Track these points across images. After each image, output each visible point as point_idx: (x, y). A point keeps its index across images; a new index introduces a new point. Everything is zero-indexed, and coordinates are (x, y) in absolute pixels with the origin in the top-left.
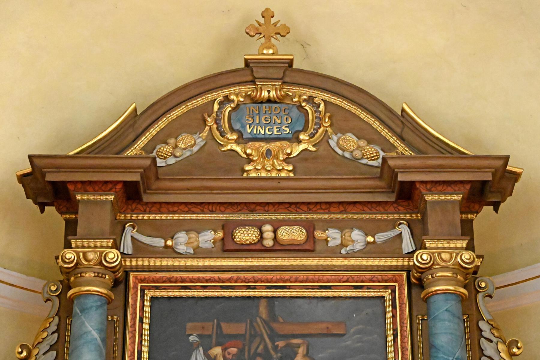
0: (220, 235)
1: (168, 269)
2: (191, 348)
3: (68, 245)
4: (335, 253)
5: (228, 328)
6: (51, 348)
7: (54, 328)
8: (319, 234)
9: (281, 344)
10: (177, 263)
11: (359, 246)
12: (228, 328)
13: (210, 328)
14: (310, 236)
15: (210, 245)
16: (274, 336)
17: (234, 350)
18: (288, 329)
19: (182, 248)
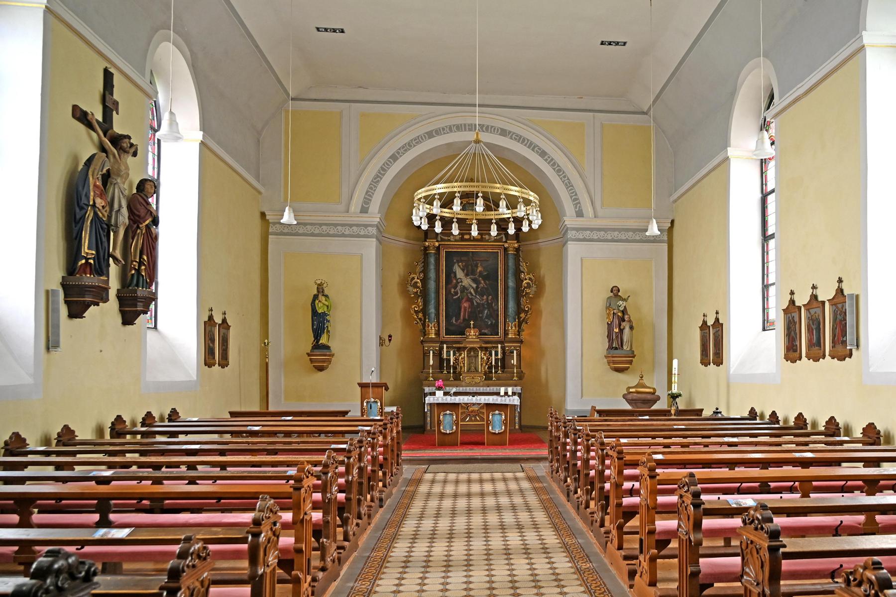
0: (461, 236)
1: (447, 245)
2: (455, 263)
3: (426, 241)
4: (487, 241)
5: (463, 259)
6: (422, 263)
7: (423, 258)
8: (483, 236)
9: (475, 262)
10: (452, 243)
11: (493, 240)
12: (463, 259)
13: (459, 258)
14: (482, 237)
15: (458, 239)
16: (473, 261)
17: (464, 264)
18: (477, 259)
19: (452, 240)
